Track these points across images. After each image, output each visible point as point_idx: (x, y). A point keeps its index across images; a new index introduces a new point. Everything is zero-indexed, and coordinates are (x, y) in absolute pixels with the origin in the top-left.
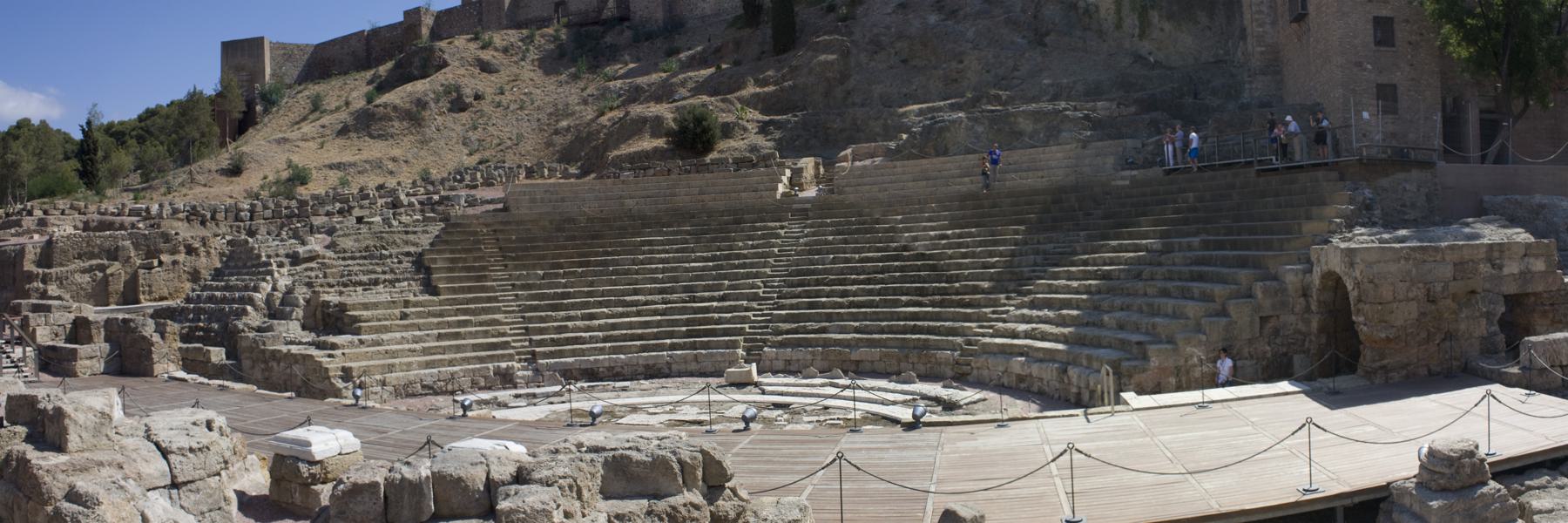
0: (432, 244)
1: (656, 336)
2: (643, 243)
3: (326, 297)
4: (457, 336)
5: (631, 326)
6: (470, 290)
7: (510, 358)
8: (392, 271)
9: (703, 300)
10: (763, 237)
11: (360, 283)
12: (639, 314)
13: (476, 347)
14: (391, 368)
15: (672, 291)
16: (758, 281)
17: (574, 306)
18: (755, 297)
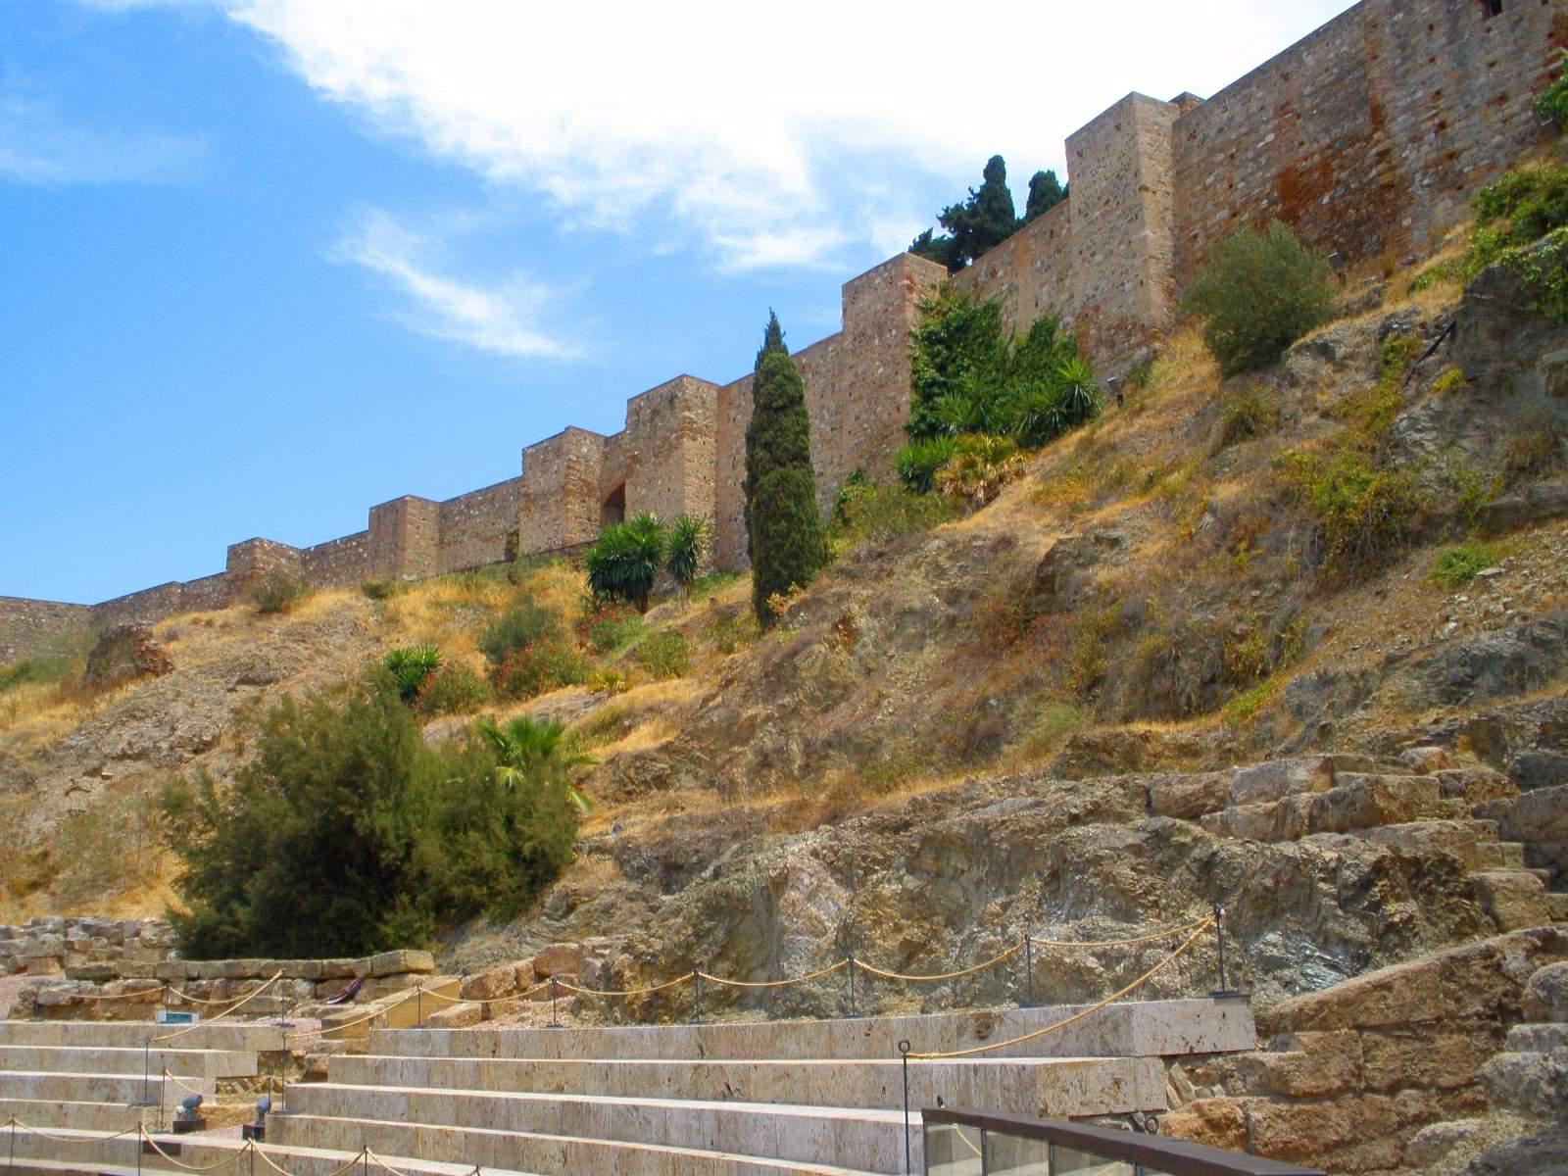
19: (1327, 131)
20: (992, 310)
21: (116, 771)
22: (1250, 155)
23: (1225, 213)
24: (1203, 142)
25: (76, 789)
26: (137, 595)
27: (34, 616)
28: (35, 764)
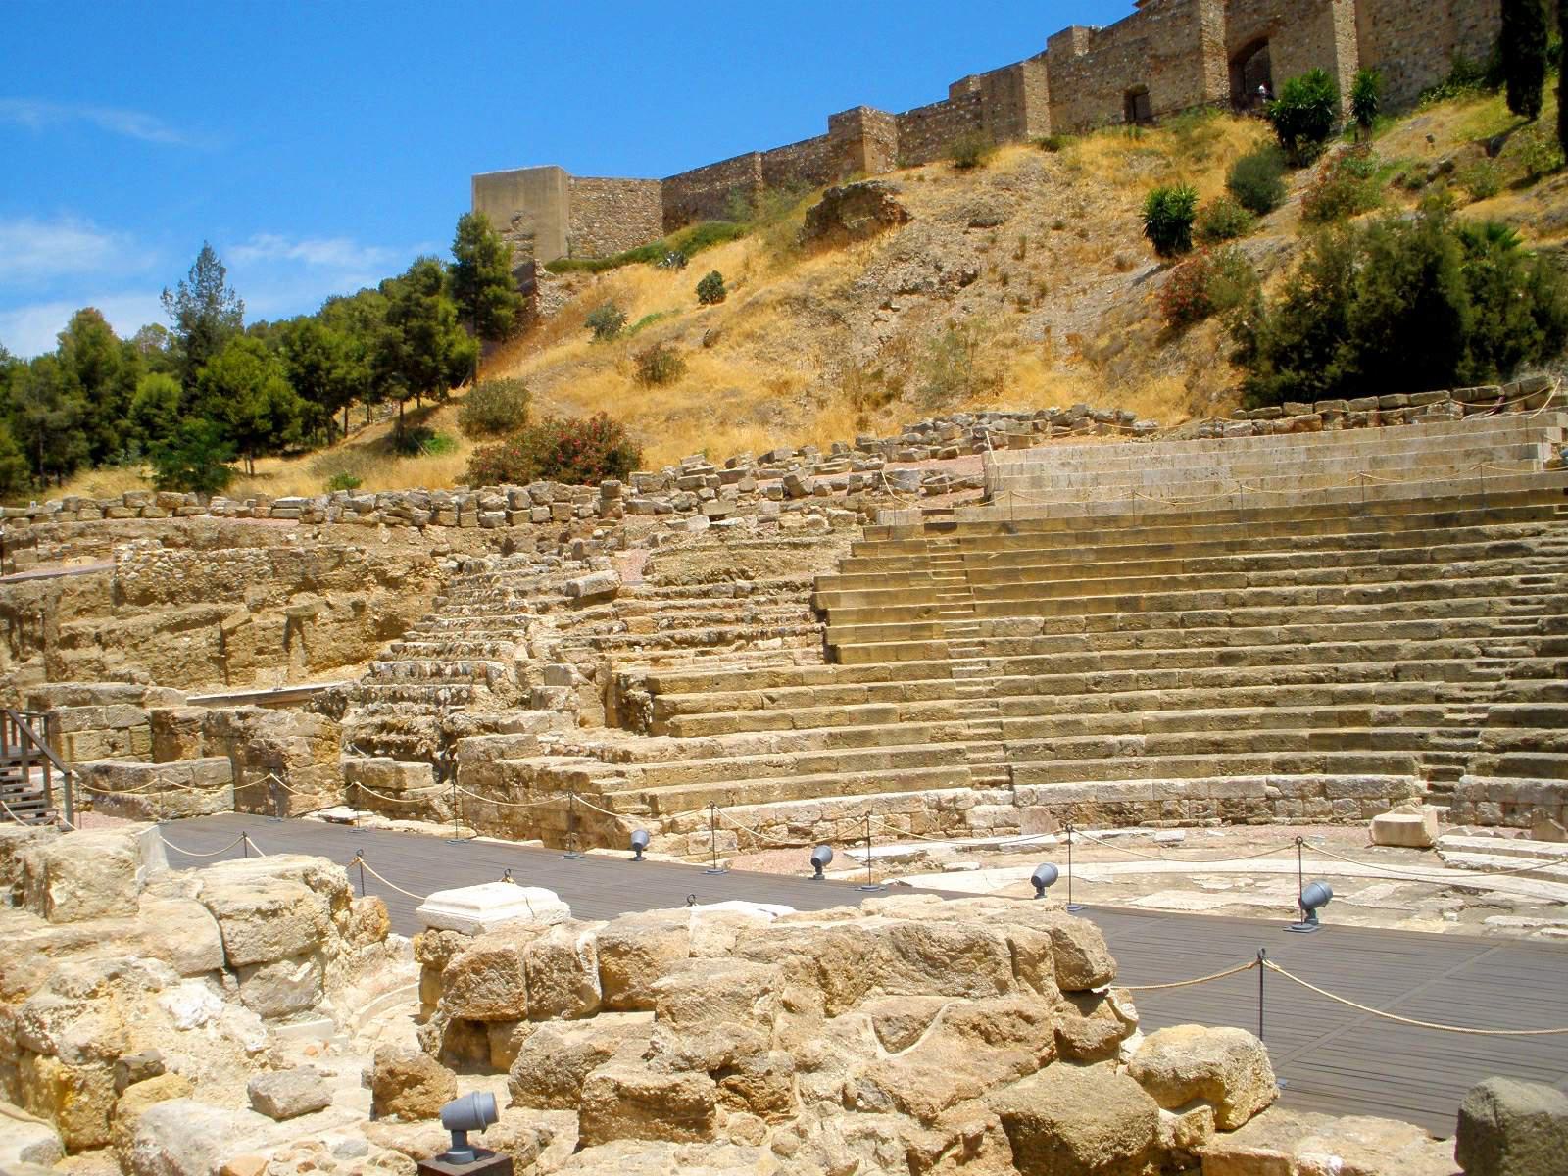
0: (841, 565)
1: (1252, 745)
2: (1248, 565)
3: (625, 669)
4: (863, 738)
5: (1201, 723)
6: (897, 652)
7: (960, 780)
8: (755, 619)
9: (1353, 678)
10: (1495, 552)
11: (691, 642)
12: (1223, 702)
13: (896, 760)
14: (731, 798)
15: (1296, 658)
16: (1468, 643)
18: (1457, 674)
21: (904, 303)
25: (878, 320)
27: (611, 192)
28: (835, 302)
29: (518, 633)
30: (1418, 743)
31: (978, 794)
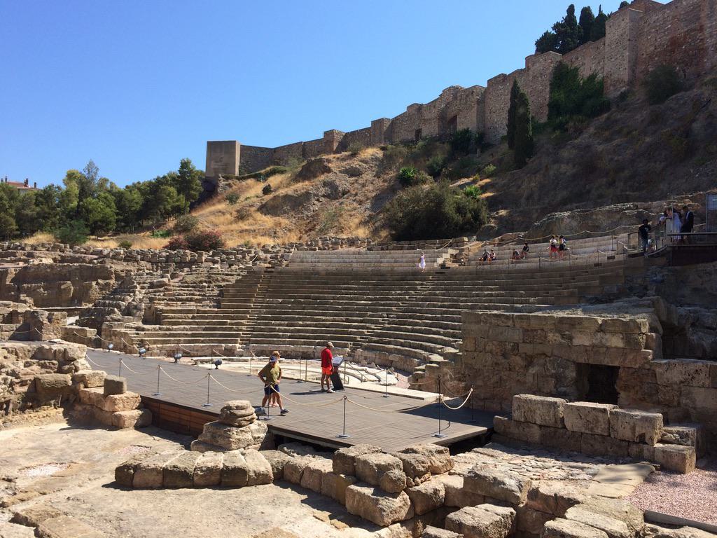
2: (345, 289)
13: (221, 335)
17: (286, 319)
19: (687, 26)
20: (576, 69)
22: (663, 31)
23: (653, 48)
24: (649, 25)
26: (289, 145)
29: (132, 294)
30: (354, 340)
31: (240, 346)
